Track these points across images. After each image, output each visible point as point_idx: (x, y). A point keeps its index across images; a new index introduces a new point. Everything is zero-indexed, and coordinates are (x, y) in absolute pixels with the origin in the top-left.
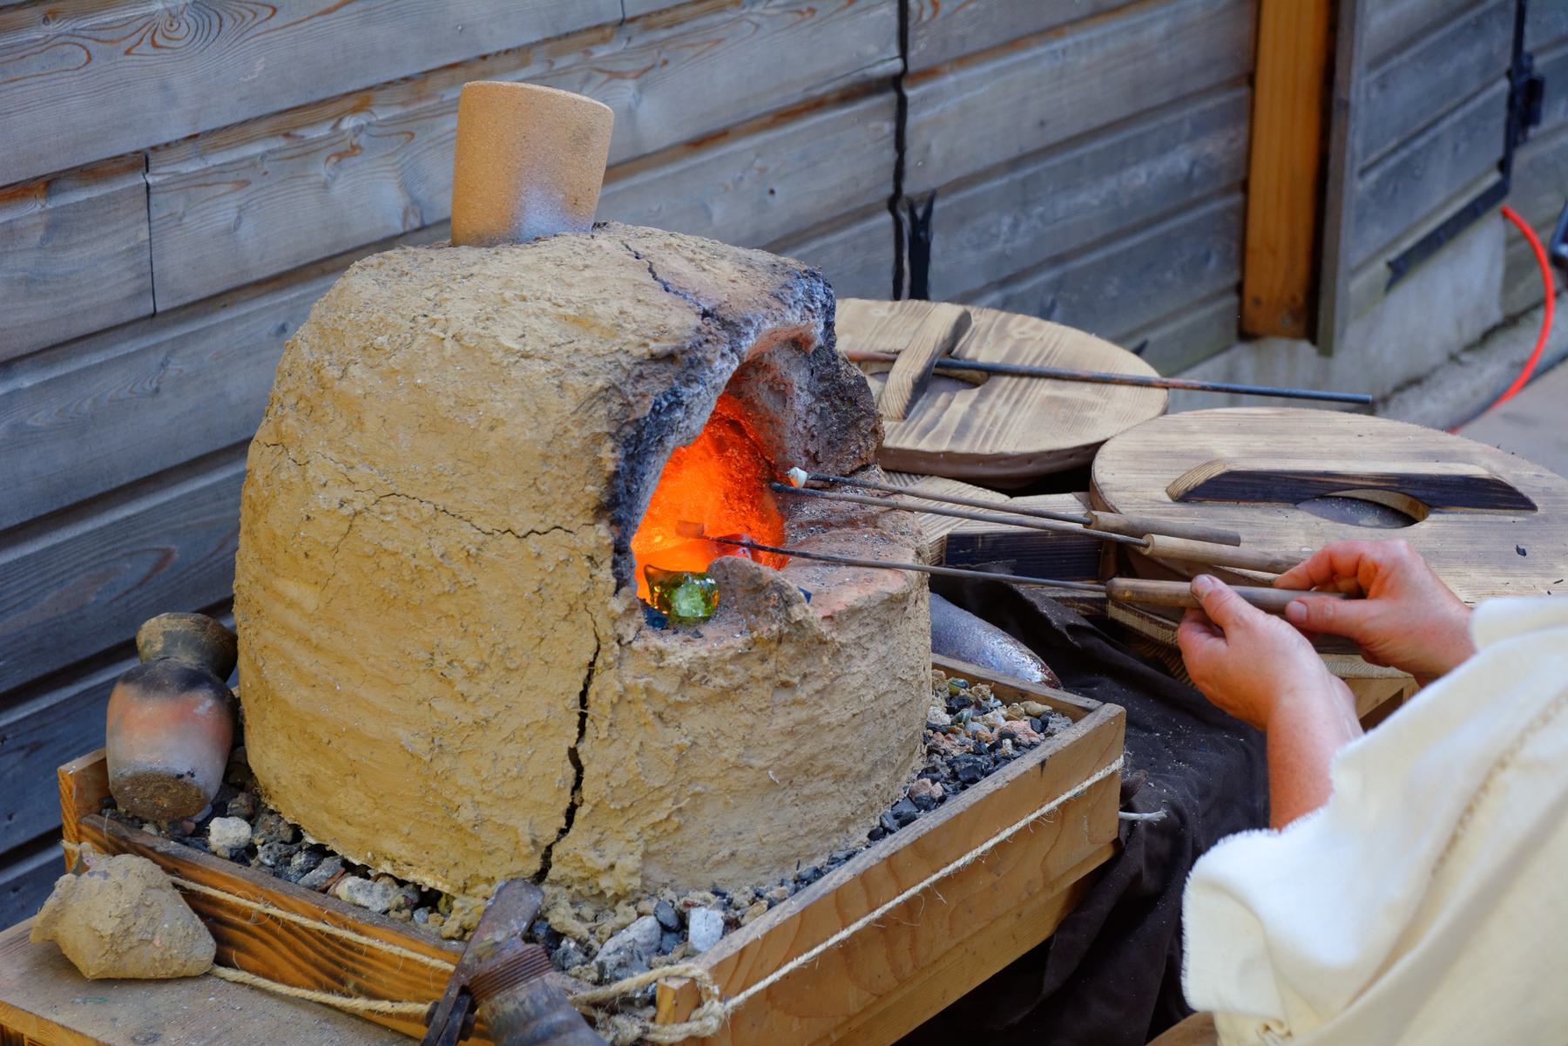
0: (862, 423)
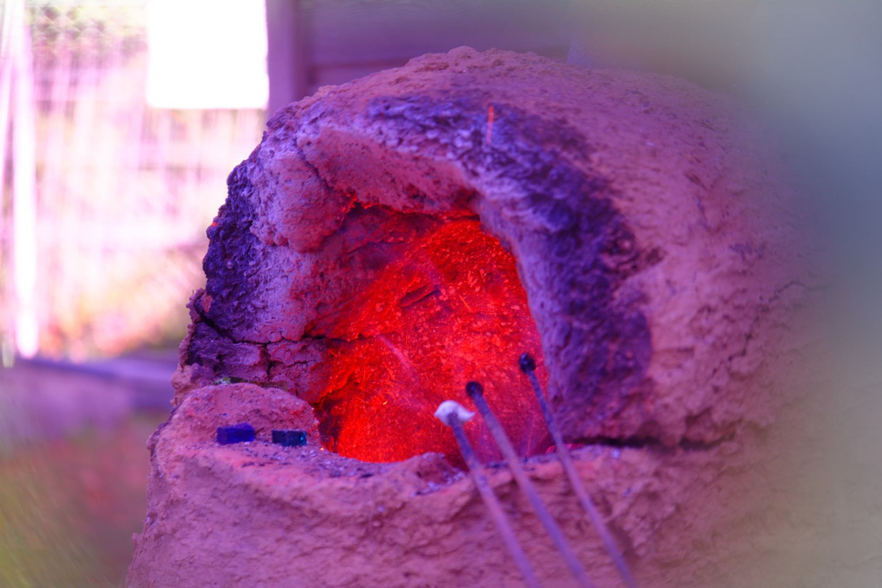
0: (629, 380)
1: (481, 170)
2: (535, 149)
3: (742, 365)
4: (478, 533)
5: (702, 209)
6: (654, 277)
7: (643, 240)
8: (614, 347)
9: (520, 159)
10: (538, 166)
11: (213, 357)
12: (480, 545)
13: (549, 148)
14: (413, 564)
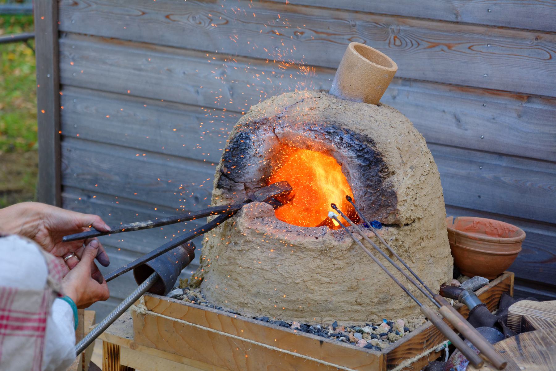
0: (389, 208)
1: (341, 147)
2: (360, 144)
3: (416, 203)
4: (353, 253)
5: (402, 158)
6: (394, 179)
7: (391, 170)
8: (383, 199)
9: (355, 146)
10: (361, 148)
11: (228, 187)
12: (354, 256)
13: (364, 143)
14: (335, 262)
